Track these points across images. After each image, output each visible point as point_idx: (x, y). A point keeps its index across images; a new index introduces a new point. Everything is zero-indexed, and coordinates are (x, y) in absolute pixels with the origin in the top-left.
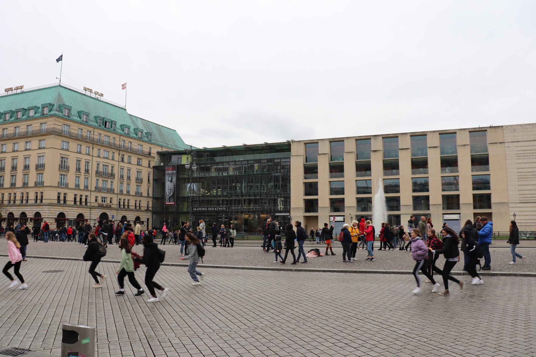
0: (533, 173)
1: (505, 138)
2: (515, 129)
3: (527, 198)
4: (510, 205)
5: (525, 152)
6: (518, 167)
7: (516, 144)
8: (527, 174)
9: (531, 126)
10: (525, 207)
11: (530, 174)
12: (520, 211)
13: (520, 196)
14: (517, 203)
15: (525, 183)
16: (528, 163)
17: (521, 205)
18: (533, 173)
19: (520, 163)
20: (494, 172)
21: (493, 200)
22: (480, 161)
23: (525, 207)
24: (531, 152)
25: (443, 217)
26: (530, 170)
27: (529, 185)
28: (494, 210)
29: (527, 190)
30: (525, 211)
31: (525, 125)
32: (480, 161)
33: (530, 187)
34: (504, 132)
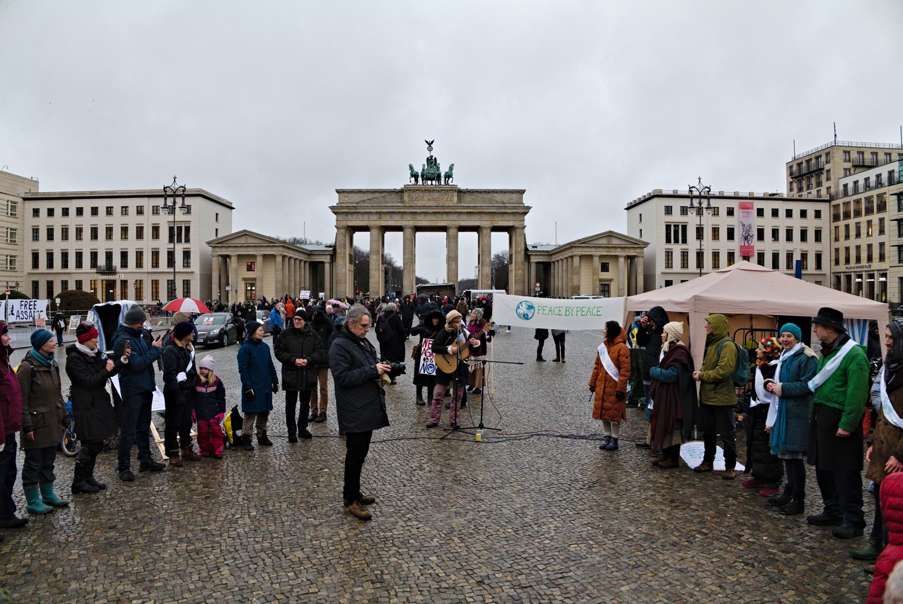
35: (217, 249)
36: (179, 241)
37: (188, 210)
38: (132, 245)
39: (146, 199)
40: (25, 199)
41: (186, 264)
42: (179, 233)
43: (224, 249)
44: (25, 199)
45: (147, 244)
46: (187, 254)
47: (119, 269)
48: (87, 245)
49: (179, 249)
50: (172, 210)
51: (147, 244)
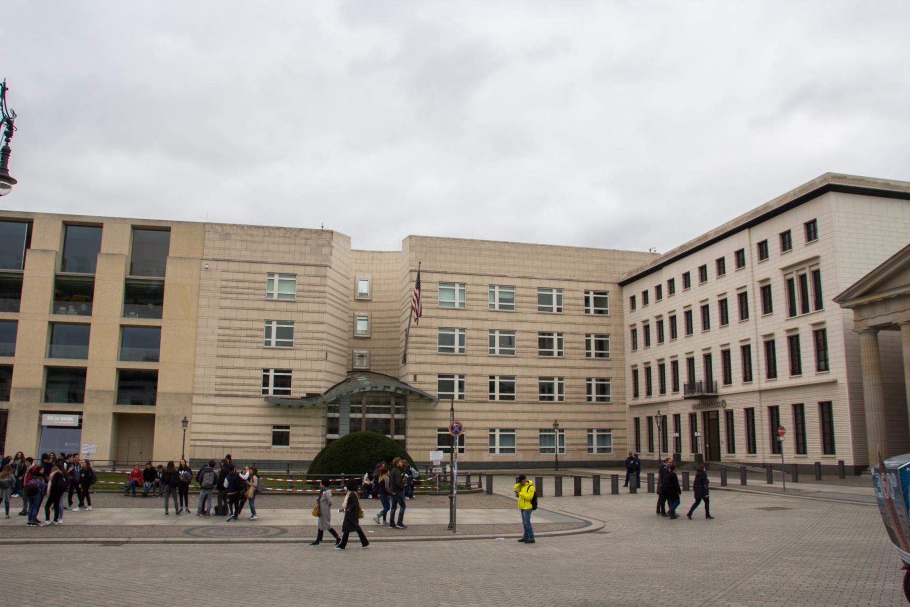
0: (249, 333)
1: (206, 251)
2: (228, 234)
3: (232, 385)
4: (196, 399)
5: (241, 284)
6: (223, 316)
7: (224, 265)
8: (238, 332)
9: (261, 232)
10: (226, 406)
11: (244, 333)
12: (214, 414)
13: (219, 380)
14: (210, 395)
15: (232, 352)
16: (242, 309)
17: (217, 400)
18: (249, 333)
19: (226, 308)
20: (172, 322)
21: (162, 386)
22: (144, 295)
23: (226, 406)
24: (252, 285)
25: (40, 419)
26: (245, 324)
27: (239, 357)
28: (159, 409)
29: (234, 368)
30: (225, 415)
31: (250, 227)
32: (144, 295)
33: (240, 363)
34: (207, 236)
35: (866, 313)
36: (805, 309)
37: (811, 230)
38: (735, 334)
39: (746, 232)
40: (623, 284)
41: (822, 364)
42: (805, 289)
43: (880, 310)
44: (623, 284)
45: (756, 328)
46: (820, 337)
47: (722, 390)
48: (679, 348)
49: (804, 326)
50: (786, 240)
51: (756, 328)
